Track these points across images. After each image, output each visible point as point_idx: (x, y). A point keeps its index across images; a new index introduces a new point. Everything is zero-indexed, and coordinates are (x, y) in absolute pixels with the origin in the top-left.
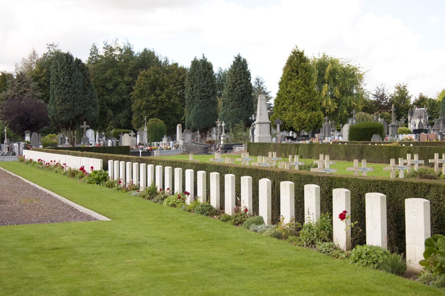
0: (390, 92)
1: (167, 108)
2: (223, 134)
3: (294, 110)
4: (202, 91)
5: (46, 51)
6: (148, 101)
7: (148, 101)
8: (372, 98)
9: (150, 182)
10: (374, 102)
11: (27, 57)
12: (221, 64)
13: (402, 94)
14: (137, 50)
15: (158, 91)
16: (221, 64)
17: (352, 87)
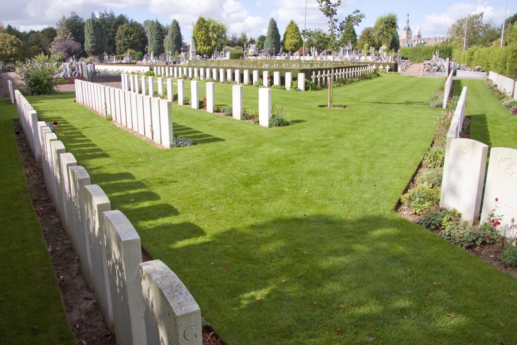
0: (239, 36)
1: (133, 44)
2: (170, 56)
3: (201, 45)
4: (157, 36)
5: (71, 16)
6: (124, 41)
7: (124, 41)
8: (230, 39)
9: (23, 107)
10: (232, 41)
11: (61, 19)
12: (155, 20)
13: (244, 36)
14: (117, 15)
15: (129, 36)
16: (155, 20)
17: (222, 33)
